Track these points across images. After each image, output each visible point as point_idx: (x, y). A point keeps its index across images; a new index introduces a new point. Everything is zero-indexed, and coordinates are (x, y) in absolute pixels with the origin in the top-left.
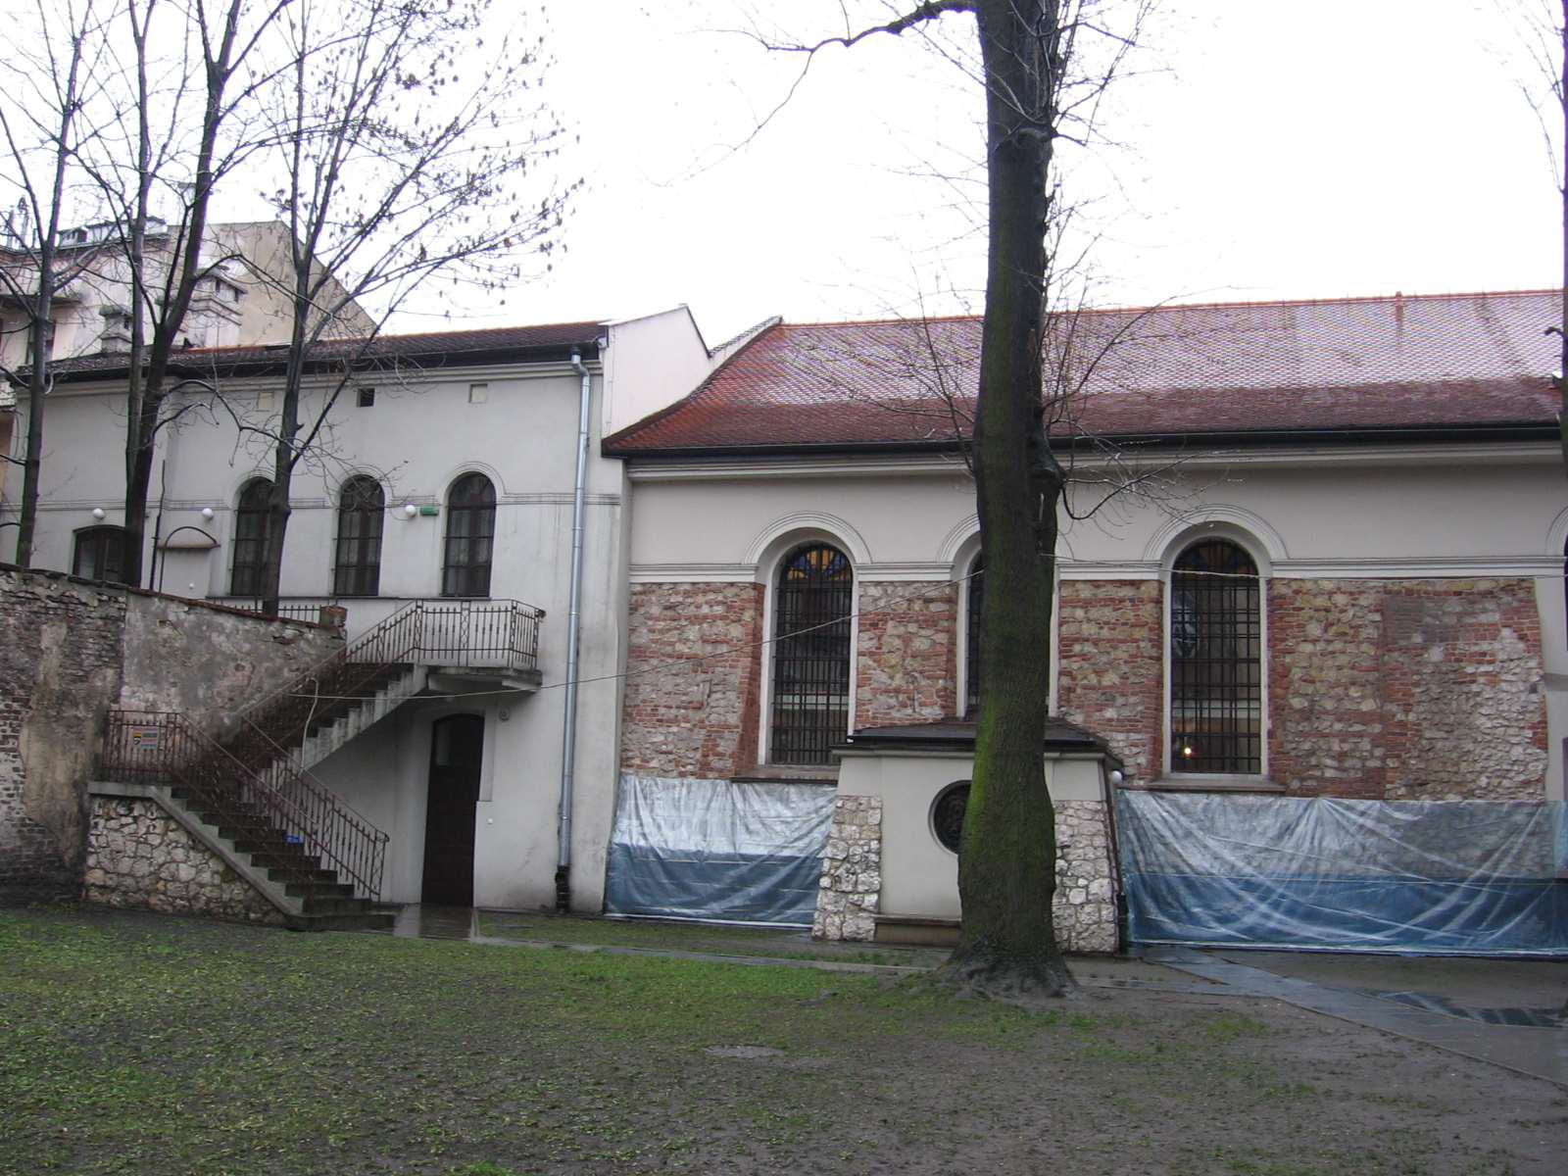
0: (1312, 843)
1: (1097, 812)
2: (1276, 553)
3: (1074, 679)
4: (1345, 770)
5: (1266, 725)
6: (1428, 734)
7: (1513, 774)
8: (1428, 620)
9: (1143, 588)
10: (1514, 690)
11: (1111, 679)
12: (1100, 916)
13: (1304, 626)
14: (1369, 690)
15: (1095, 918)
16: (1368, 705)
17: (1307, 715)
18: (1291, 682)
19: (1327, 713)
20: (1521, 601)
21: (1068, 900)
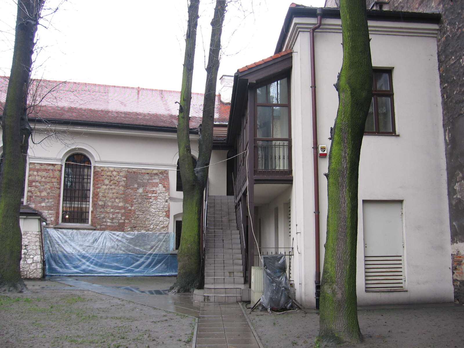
0: (103, 244)
1: (37, 235)
2: (97, 158)
3: (32, 193)
4: (113, 223)
5: (91, 209)
6: (137, 213)
7: (160, 225)
8: (139, 180)
9: (56, 167)
10: (161, 201)
11: (44, 194)
12: (37, 267)
13: (104, 180)
14: (121, 200)
16: (121, 204)
17: (103, 207)
18: (99, 197)
19: (109, 206)
20: (165, 177)
21: (27, 263)
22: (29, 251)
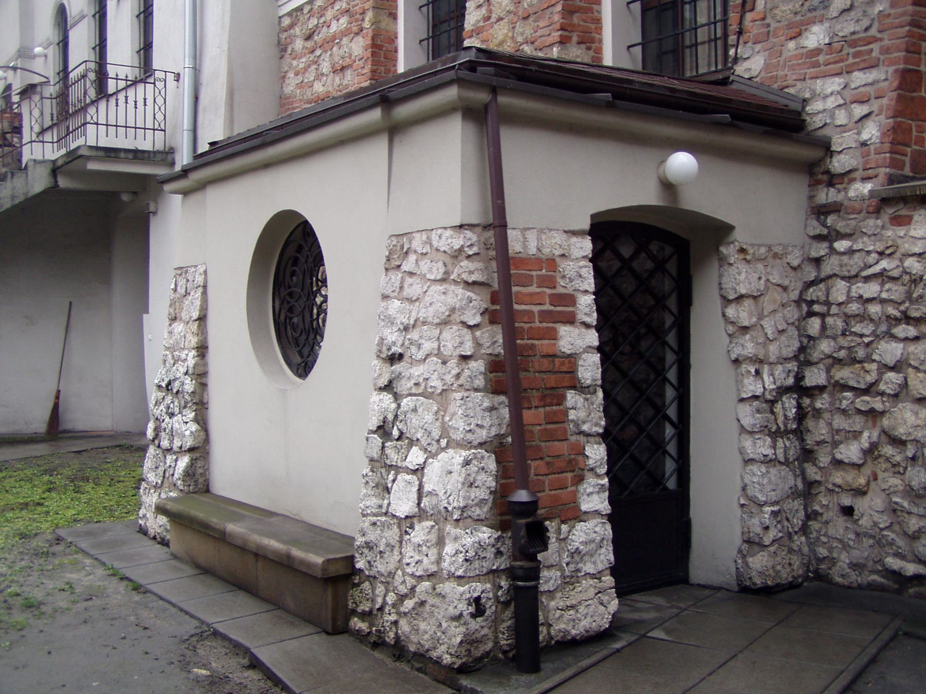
1: (457, 255)
15: (428, 564)
22: (406, 403)
